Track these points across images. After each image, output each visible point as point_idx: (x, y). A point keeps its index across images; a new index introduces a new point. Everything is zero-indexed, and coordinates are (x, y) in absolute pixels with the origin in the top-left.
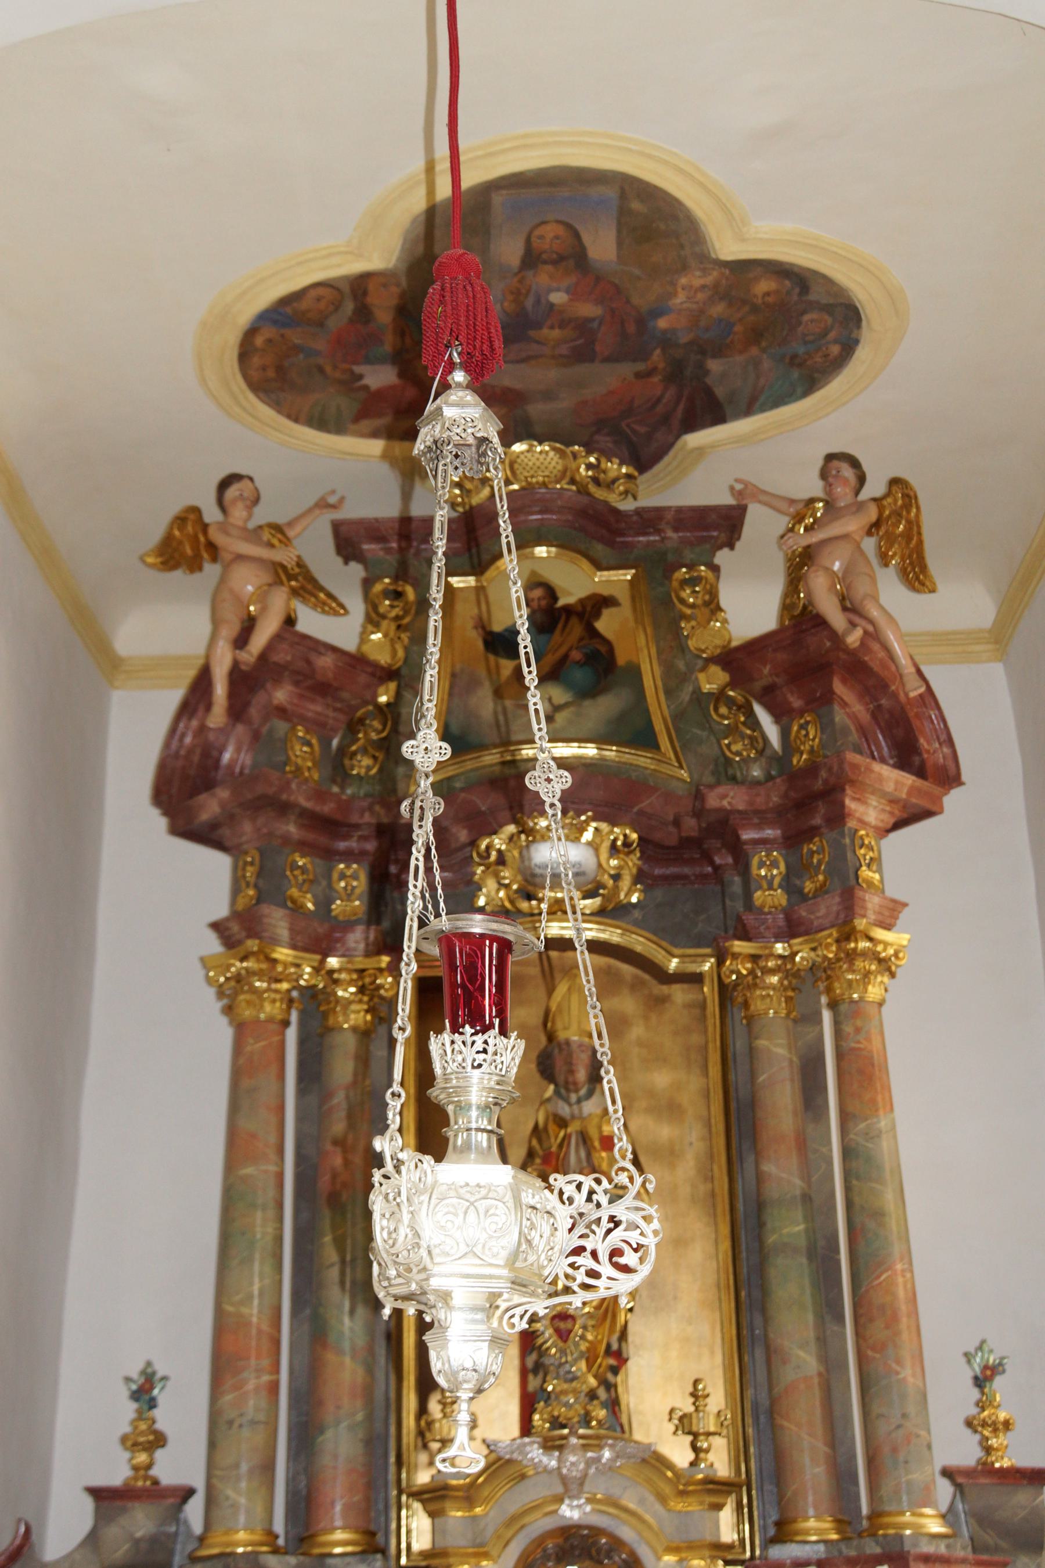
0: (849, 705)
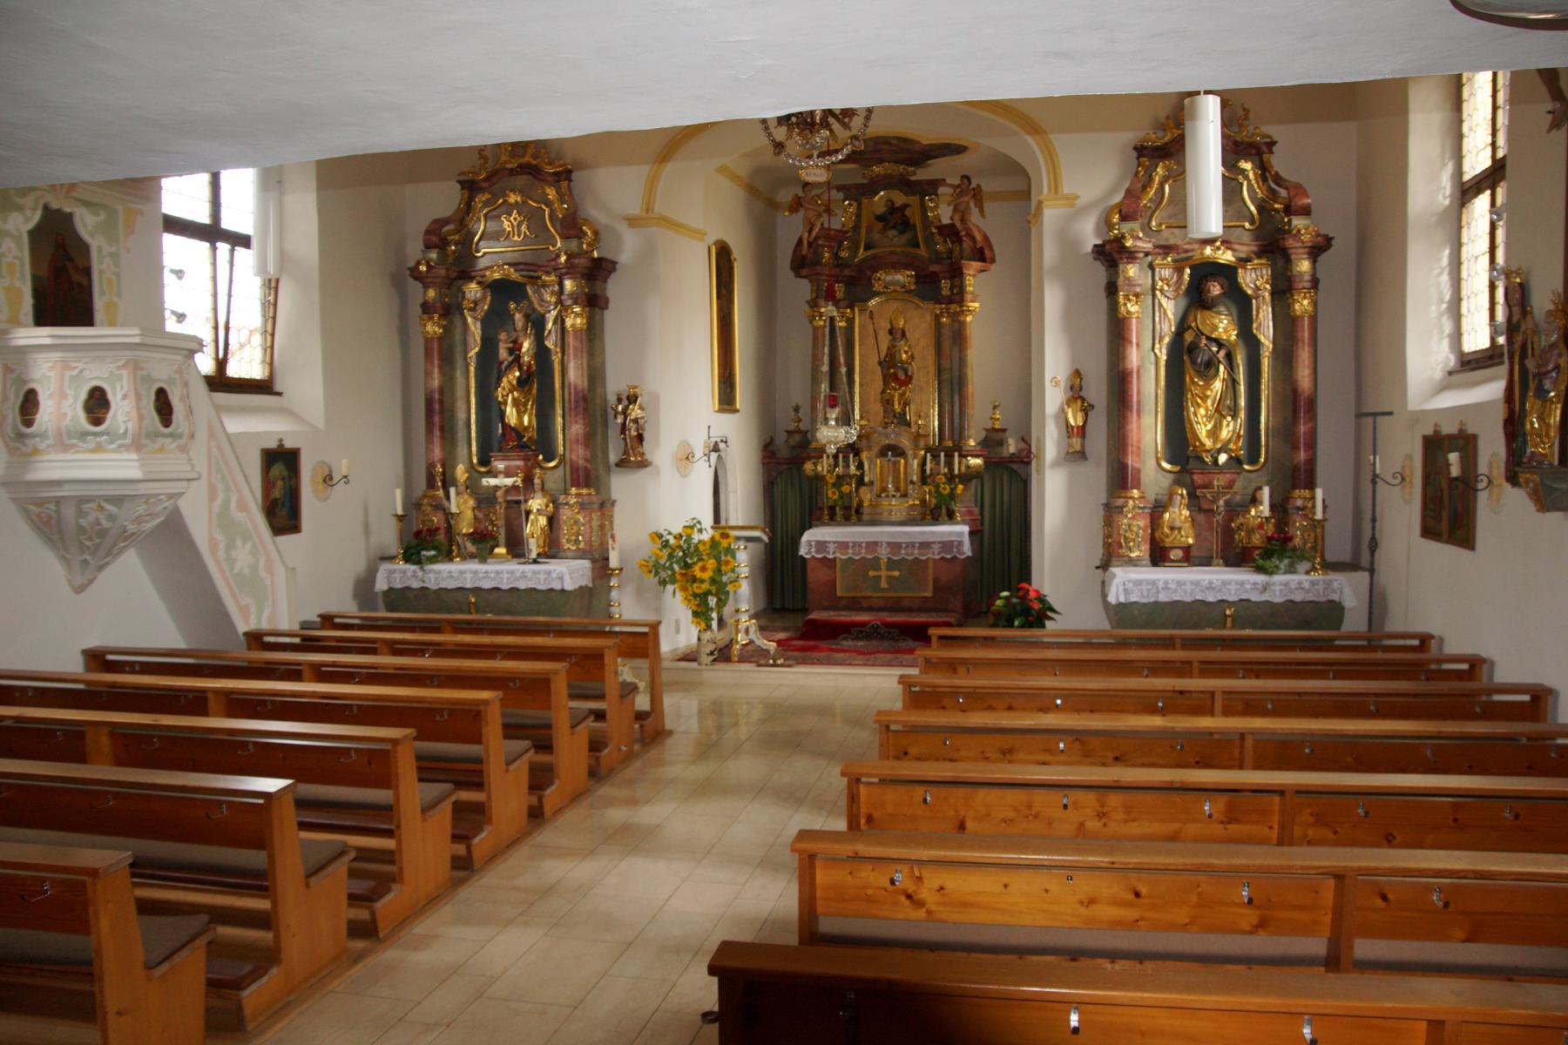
0: (967, 244)
